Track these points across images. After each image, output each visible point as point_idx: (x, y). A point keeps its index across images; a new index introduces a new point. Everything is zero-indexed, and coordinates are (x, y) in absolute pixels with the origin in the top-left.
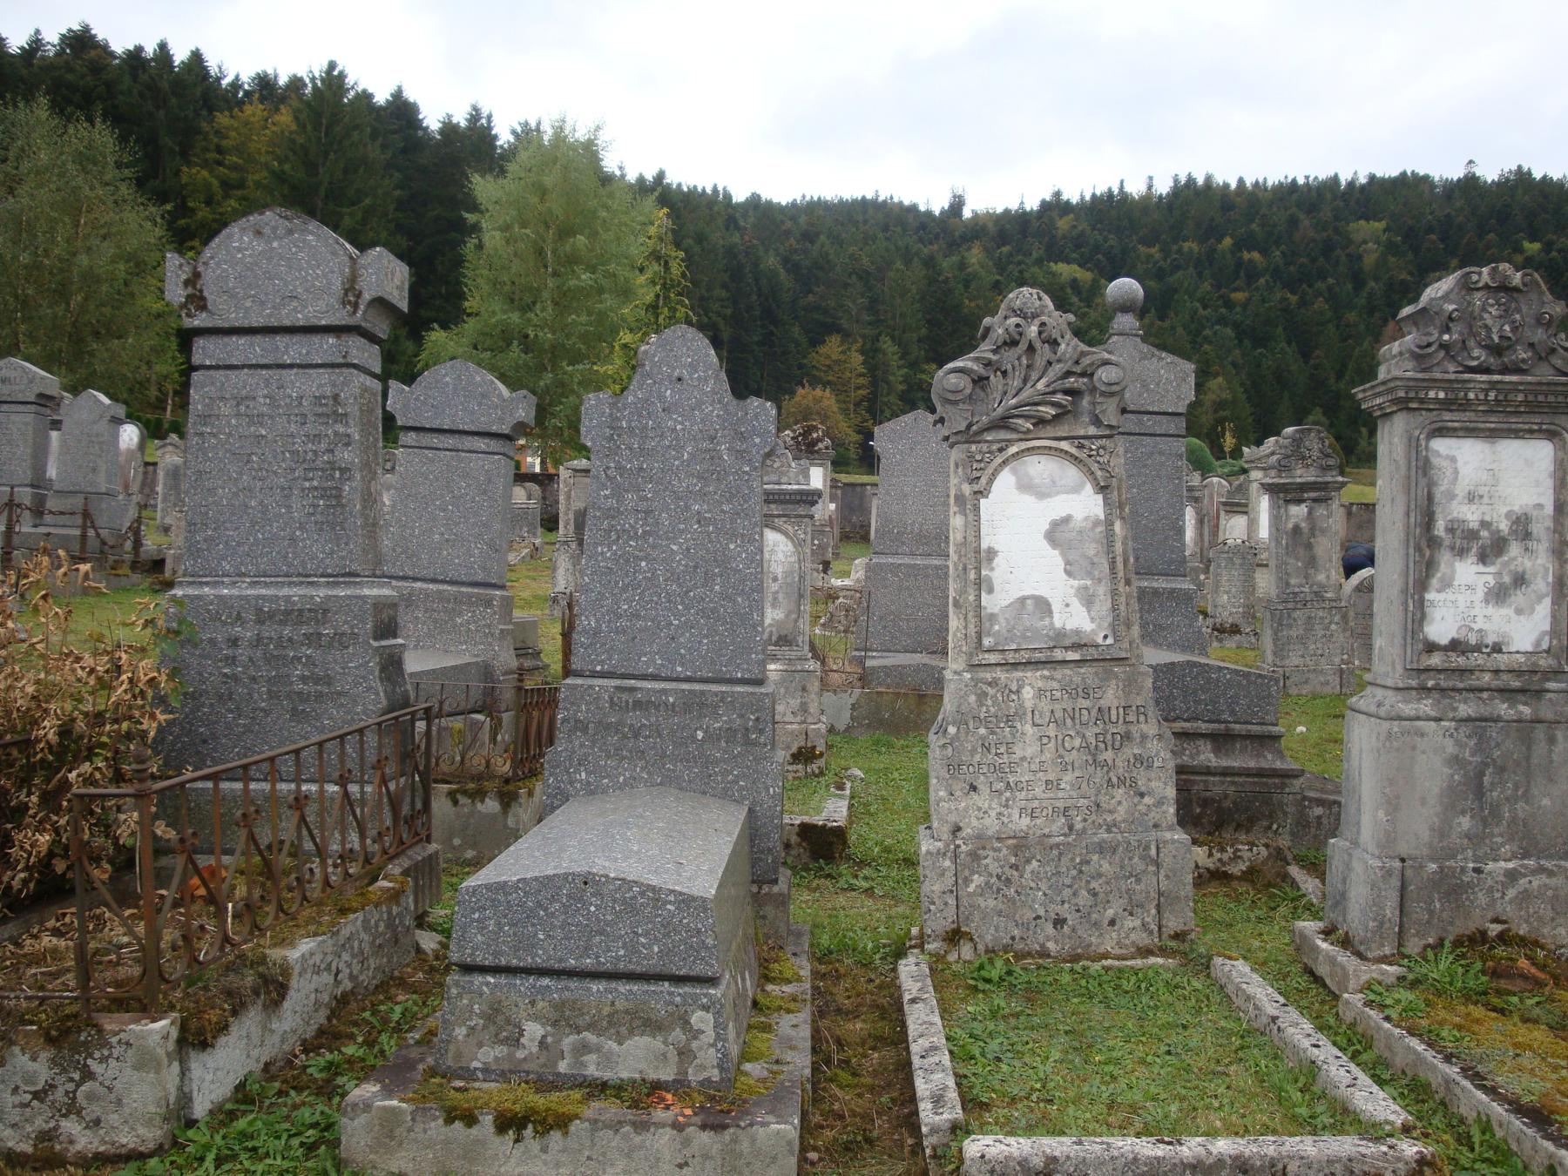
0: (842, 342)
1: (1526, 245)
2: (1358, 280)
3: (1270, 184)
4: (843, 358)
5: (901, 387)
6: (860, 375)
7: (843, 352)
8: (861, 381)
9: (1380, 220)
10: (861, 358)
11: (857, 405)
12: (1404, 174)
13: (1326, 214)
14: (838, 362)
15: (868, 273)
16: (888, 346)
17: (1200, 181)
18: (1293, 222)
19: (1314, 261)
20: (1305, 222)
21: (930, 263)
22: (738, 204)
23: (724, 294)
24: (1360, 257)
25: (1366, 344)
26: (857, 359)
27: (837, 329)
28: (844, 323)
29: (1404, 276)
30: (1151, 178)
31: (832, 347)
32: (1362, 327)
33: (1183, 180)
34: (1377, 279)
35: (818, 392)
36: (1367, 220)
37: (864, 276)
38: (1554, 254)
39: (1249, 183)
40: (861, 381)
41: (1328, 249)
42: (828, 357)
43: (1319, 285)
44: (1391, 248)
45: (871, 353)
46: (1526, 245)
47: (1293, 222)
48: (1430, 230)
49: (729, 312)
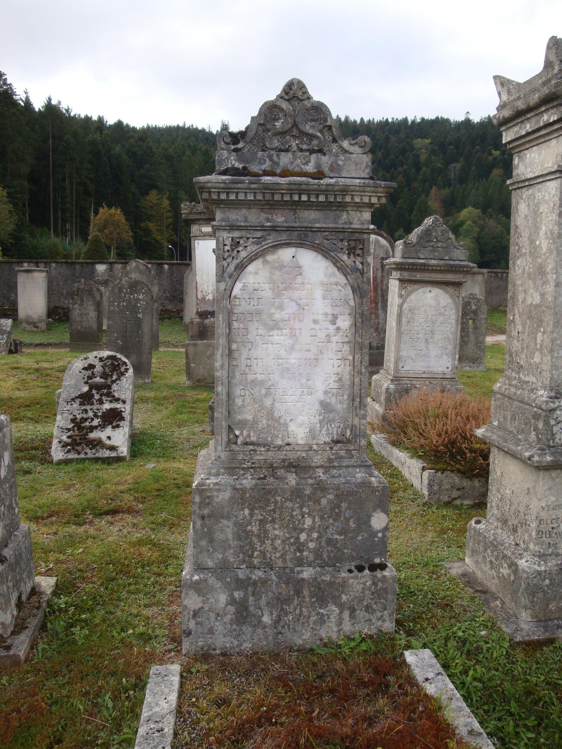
1: (493, 151)
2: (418, 166)
3: (376, 121)
4: (159, 202)
7: (159, 199)
8: (169, 214)
10: (168, 202)
11: (168, 227)
12: (437, 118)
13: (402, 135)
15: (172, 157)
17: (343, 119)
18: (387, 139)
19: (397, 157)
20: (393, 139)
23: (89, 166)
24: (418, 156)
25: (423, 196)
26: (166, 203)
27: (156, 187)
28: (159, 184)
29: (439, 165)
31: (153, 196)
32: (420, 189)
34: (427, 167)
35: (113, 210)
36: (422, 139)
37: (169, 158)
38: (506, 156)
39: (366, 120)
40: (169, 214)
41: (403, 152)
43: (400, 169)
44: (433, 152)
46: (493, 151)
47: (387, 139)
48: (450, 144)
49: (92, 176)
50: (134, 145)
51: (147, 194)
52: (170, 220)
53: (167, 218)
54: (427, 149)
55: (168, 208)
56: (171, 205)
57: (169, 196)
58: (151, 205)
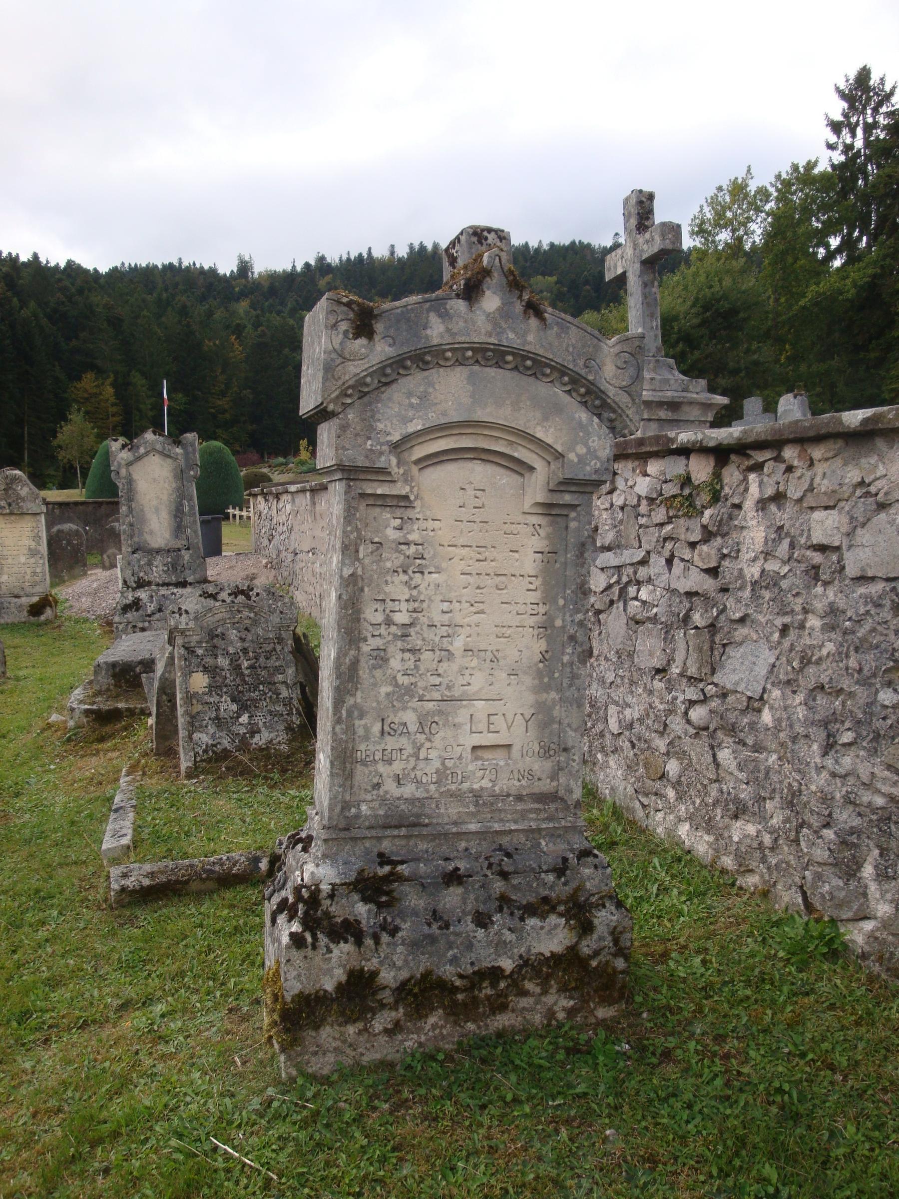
0: (96, 379)
5: (150, 414)
6: (113, 405)
9: (551, 275)
12: (573, 243)
14: (96, 395)
16: (138, 380)
17: (430, 247)
21: (184, 311)
22: (23, 263)
26: (109, 391)
27: (93, 367)
30: (393, 246)
31: (88, 381)
33: (417, 247)
37: (115, 322)
42: (86, 391)
45: (122, 387)
50: (63, 303)
51: (79, 379)
52: (117, 419)
53: (113, 416)
54: (551, 292)
55: (113, 399)
56: (117, 394)
57: (116, 380)
58: (86, 395)
